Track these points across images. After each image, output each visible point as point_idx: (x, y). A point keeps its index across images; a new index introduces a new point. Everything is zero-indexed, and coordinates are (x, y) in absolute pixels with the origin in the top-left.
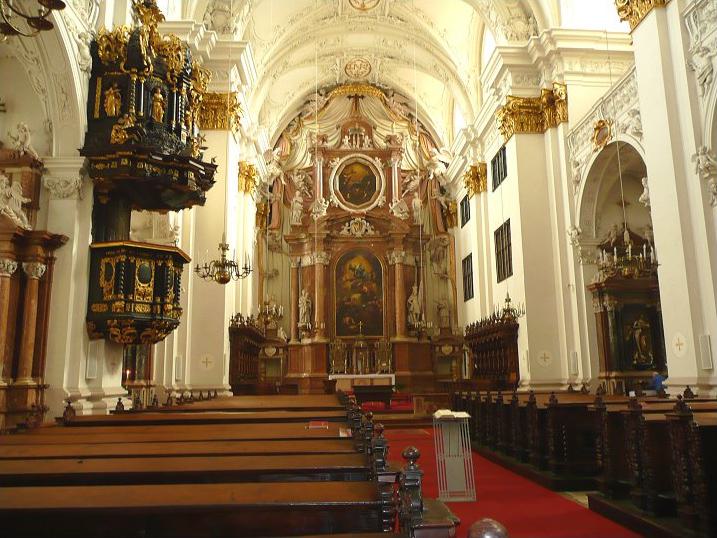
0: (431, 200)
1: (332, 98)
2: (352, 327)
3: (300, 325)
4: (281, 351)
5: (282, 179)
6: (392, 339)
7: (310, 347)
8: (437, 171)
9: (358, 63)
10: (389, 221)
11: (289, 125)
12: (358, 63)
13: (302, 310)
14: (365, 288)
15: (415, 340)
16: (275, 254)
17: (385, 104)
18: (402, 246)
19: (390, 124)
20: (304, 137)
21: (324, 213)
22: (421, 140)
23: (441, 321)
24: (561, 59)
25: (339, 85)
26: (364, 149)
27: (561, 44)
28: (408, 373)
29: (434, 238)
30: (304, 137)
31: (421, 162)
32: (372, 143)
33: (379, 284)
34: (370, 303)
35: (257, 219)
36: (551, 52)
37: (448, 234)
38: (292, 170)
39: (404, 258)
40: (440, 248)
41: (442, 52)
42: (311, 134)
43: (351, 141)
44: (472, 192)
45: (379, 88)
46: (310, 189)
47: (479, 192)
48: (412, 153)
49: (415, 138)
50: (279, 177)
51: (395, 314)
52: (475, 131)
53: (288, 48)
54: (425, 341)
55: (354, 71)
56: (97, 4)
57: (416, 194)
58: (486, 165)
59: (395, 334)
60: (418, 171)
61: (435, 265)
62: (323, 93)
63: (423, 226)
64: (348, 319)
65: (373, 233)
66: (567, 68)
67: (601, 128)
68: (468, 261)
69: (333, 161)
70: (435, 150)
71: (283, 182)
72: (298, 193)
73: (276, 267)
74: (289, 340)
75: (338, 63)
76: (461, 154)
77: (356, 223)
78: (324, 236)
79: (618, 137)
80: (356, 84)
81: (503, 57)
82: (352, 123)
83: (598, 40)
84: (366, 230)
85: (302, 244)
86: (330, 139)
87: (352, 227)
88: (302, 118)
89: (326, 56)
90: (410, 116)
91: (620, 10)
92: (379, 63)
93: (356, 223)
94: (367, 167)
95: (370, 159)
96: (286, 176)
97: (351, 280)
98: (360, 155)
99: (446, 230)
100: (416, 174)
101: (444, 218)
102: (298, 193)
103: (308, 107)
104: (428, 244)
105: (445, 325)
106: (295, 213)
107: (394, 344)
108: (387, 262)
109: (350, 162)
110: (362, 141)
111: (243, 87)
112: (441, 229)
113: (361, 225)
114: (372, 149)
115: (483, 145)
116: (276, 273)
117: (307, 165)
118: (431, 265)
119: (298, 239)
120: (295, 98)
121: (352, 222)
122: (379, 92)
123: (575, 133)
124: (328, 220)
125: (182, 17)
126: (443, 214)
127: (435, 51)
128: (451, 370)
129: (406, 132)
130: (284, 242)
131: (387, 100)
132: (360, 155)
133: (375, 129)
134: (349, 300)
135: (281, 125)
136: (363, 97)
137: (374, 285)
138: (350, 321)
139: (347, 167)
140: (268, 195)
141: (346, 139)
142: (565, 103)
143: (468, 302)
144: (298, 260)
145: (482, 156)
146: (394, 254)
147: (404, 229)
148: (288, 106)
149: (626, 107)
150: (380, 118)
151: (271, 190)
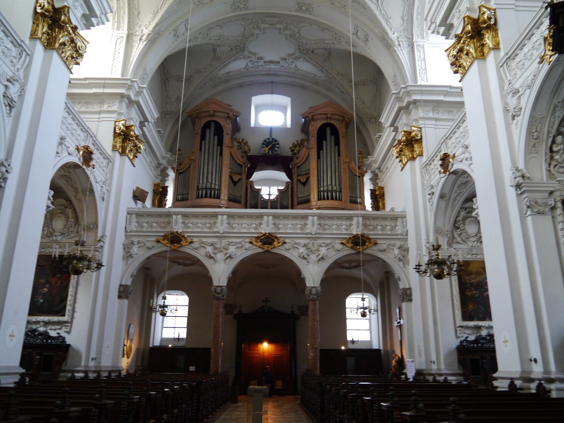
24: (417, 108)
27: (415, 97)
36: (409, 104)
56: (28, 55)
66: (421, 115)
67: (445, 158)
79: (457, 166)
83: (447, 94)
91: (452, 64)
123: (428, 164)
125: (122, 76)
142: (420, 141)
149: (461, 143)
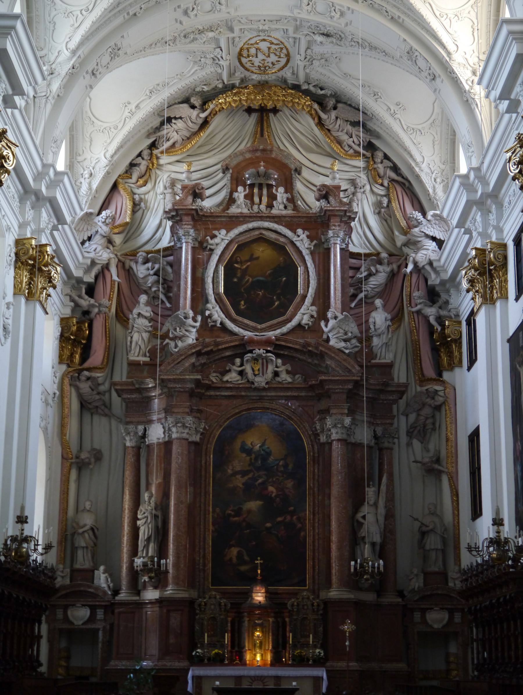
0: (409, 312)
1: (214, 113)
2: (243, 568)
3: (138, 562)
4: (100, 614)
5: (113, 270)
6: (323, 595)
7: (157, 609)
8: (421, 257)
9: (264, 46)
10: (322, 356)
11: (132, 165)
12: (264, 46)
13: (144, 532)
14: (271, 489)
15: (370, 597)
16: (96, 418)
17: (320, 124)
18: (346, 405)
19: (327, 162)
20: (160, 188)
21: (191, 338)
22: (393, 196)
23: (425, 558)
25: (228, 88)
26: (274, 212)
28: (353, 665)
29: (415, 389)
30: (160, 188)
31: (392, 239)
32: (292, 200)
33: (301, 482)
34: (279, 519)
35: (62, 348)
37: (443, 382)
38: (133, 254)
39: (349, 430)
40: (427, 411)
41: (419, 24)
42: (173, 183)
43: (249, 197)
44: (479, 300)
45: (307, 93)
46: (168, 290)
47: (493, 302)
48: (373, 221)
49: (381, 191)
50: (106, 267)
51: (329, 541)
52: (483, 180)
53: (119, 20)
54: (390, 598)
55: (257, 62)
57: (378, 302)
58: (505, 246)
59: (329, 585)
60: (384, 255)
61: (416, 444)
62: (196, 101)
63: (390, 366)
64: (234, 551)
65: (290, 380)
68: (475, 437)
69: (213, 237)
70: (418, 215)
71: (115, 277)
72: (143, 298)
73: (96, 446)
74: (116, 592)
75: (223, 44)
76: (461, 224)
77: (255, 360)
78: (189, 386)
80: (262, 86)
81: (514, 39)
82: (253, 163)
84: (276, 374)
85: (149, 400)
86: (208, 193)
87: (248, 368)
88: (155, 152)
89: (201, 32)
90: (370, 147)
92: (303, 45)
93: (255, 360)
94: (280, 248)
95: (288, 233)
96: (122, 265)
97: (244, 473)
98: (266, 224)
99: (440, 375)
100: (380, 263)
101: (435, 350)
102: (143, 298)
103: (167, 130)
104: (402, 402)
105: (434, 568)
106: (136, 336)
107: (327, 603)
108: (316, 435)
109: (242, 238)
110: (272, 197)
111: (17, 98)
112: (429, 372)
113: (268, 361)
114: (289, 212)
115: (500, 206)
116: (98, 456)
117: (166, 241)
118: (409, 444)
119: (139, 390)
120: (140, 115)
121: (248, 356)
122: (306, 101)
124: (199, 354)
126: (432, 341)
127: (409, 23)
128: (448, 663)
129: (363, 179)
130: (114, 394)
131: (323, 116)
132: (266, 224)
133: (298, 171)
134: (238, 512)
135: (113, 165)
136: (275, 111)
137: (290, 484)
138: (240, 555)
139: (241, 247)
140: (85, 302)
141: (240, 194)
143: (478, 521)
144: (140, 434)
145: (499, 230)
146: (329, 422)
147: (350, 371)
148: (130, 125)
150: (310, 150)
151: (91, 291)
